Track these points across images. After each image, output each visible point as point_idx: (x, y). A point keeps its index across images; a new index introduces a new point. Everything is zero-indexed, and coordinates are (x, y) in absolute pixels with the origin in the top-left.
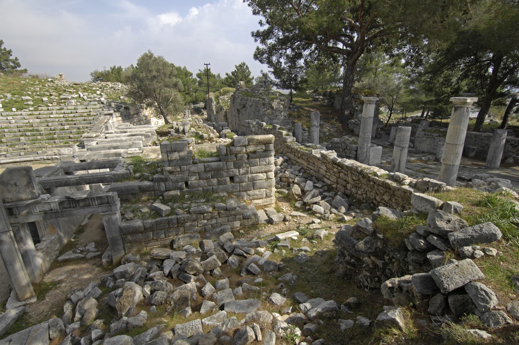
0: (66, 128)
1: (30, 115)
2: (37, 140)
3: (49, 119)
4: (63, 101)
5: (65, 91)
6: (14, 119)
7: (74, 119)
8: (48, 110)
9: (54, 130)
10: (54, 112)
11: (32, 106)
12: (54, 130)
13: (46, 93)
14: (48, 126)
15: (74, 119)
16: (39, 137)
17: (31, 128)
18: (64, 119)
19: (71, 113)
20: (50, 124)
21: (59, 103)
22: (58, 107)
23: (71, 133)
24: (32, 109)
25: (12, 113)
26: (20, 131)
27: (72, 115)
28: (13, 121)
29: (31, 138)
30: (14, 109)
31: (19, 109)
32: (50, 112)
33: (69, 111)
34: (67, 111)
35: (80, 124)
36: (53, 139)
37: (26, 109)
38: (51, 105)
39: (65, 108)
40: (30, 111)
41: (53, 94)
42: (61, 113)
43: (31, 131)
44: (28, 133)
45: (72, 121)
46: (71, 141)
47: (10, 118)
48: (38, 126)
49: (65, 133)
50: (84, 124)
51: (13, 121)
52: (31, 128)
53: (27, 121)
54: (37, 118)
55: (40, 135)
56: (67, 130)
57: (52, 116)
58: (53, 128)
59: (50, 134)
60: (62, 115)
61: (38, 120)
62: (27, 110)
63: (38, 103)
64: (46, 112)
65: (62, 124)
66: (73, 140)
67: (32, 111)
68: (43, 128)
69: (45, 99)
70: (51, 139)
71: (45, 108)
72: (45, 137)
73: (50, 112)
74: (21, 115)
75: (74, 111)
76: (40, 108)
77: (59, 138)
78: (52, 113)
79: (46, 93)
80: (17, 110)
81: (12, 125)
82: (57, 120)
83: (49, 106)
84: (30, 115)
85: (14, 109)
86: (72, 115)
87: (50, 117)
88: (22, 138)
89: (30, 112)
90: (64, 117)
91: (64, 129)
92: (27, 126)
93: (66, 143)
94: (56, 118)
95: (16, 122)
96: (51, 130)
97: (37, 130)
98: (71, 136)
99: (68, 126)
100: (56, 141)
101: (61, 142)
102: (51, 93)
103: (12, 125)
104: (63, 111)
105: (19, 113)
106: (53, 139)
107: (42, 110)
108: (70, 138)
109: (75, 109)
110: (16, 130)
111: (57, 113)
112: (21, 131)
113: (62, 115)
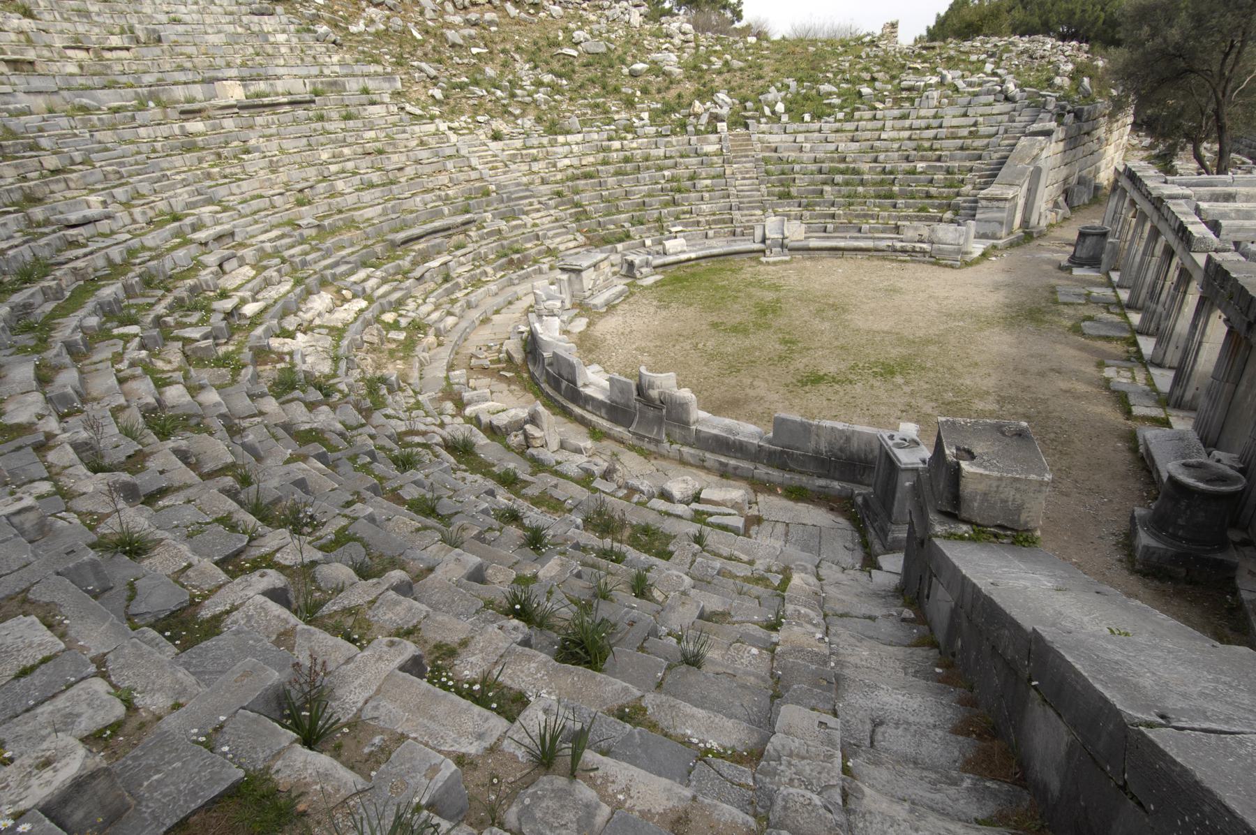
0: (919, 170)
1: (837, 131)
2: (856, 195)
3: (877, 144)
4: (904, 94)
5: (903, 66)
6: (806, 140)
7: (937, 145)
8: (874, 118)
9: (891, 173)
10: (889, 124)
11: (841, 108)
12: (891, 173)
13: (866, 76)
14: (875, 161)
15: (937, 145)
16: (860, 189)
17: (842, 166)
18: (913, 144)
19: (927, 128)
20: (882, 157)
21: (897, 102)
22: (896, 112)
23: (931, 181)
24: (840, 115)
25: (803, 127)
26: (820, 172)
27: (931, 133)
28: (808, 146)
29: (845, 190)
30: (807, 117)
31: (817, 116)
32: (879, 124)
33: (923, 123)
34: (917, 123)
35: (952, 158)
36: (890, 196)
37: (829, 115)
38: (880, 106)
39: (913, 114)
40: (836, 121)
41: (880, 75)
42: (903, 129)
43: (842, 173)
44: (839, 178)
45: (931, 149)
46: (933, 206)
47: (800, 138)
48: (854, 161)
49: (917, 181)
50: (961, 160)
51: (808, 146)
52: (842, 166)
53: (832, 147)
54: (852, 141)
55: (862, 183)
56: (921, 173)
57: (884, 136)
58: (888, 167)
59: (882, 182)
60: (906, 134)
61: (855, 146)
62: (831, 119)
63: (853, 99)
64: (870, 125)
65: (907, 159)
66: (937, 202)
67: (840, 121)
68: (865, 167)
69: (866, 90)
70: (886, 197)
71: (868, 114)
72: (872, 190)
73: (879, 124)
74: (820, 131)
75: (935, 123)
76: (857, 115)
77: (903, 194)
78: (883, 129)
79: (866, 76)
80: (813, 118)
81: (805, 156)
82: (896, 146)
83: (876, 109)
84: (837, 131)
85: (807, 117)
86: (931, 133)
87: (879, 139)
88: (827, 188)
89: (838, 125)
90: (910, 139)
91: (913, 172)
92: (832, 160)
93: (921, 210)
94: (893, 140)
95: (812, 150)
96: (884, 171)
97: (855, 172)
98: (933, 190)
99: (923, 164)
100: (900, 202)
101: (907, 206)
102: (876, 75)
103: (805, 156)
104: (907, 123)
105: (816, 125)
106: (890, 196)
107: (860, 120)
108: (929, 196)
109: (935, 117)
110: (814, 167)
111: (893, 129)
112: (824, 170)
113: (906, 134)
